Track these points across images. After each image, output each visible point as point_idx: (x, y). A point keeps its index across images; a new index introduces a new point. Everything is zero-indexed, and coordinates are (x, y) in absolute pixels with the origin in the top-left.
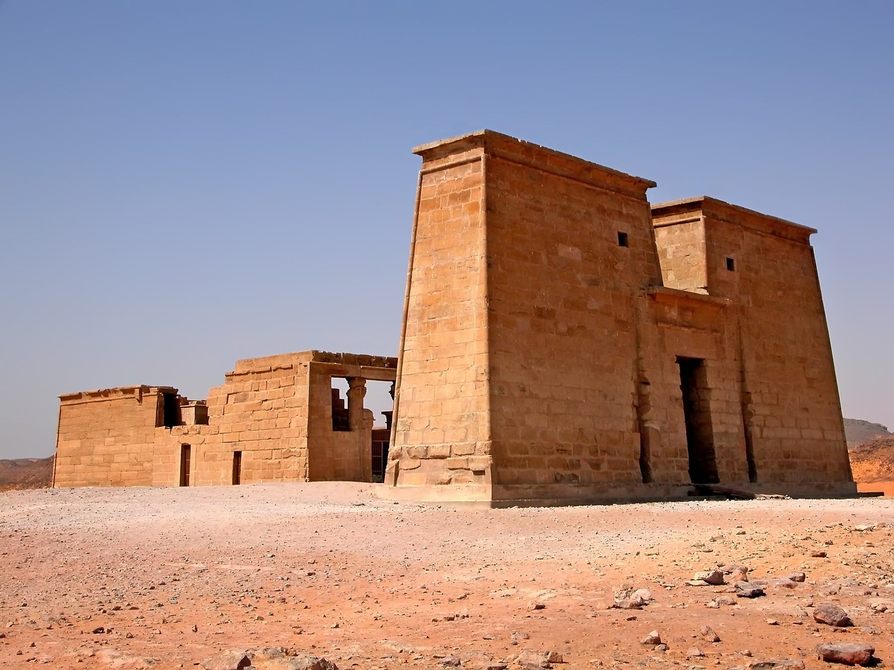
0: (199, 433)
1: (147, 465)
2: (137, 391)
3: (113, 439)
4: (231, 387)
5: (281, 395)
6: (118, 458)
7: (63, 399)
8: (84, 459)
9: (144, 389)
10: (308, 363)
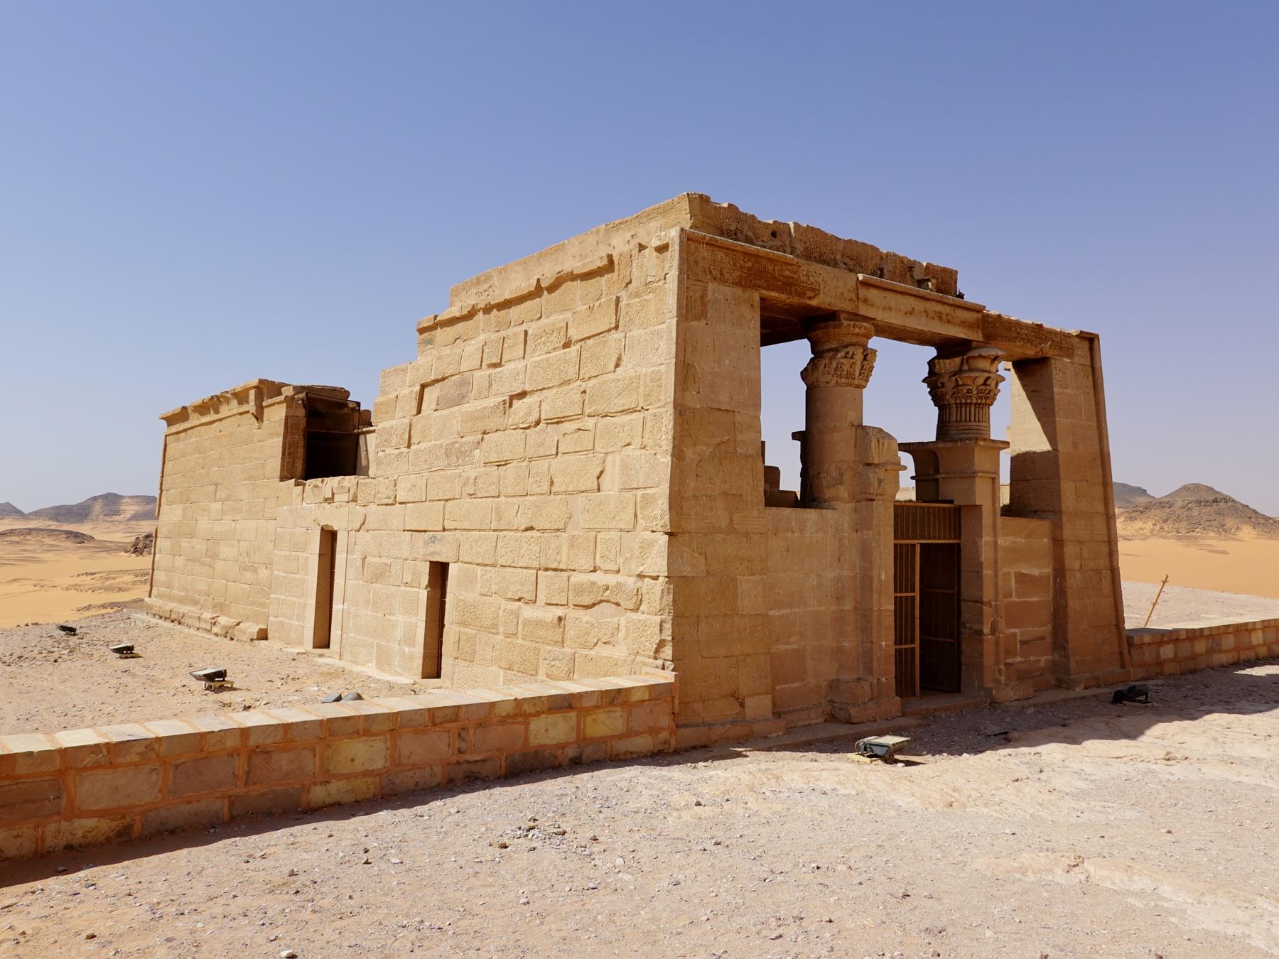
0: (354, 500)
2: (252, 393)
3: (216, 506)
4: (427, 363)
5: (572, 372)
6: (226, 551)
7: (171, 420)
8: (185, 544)
9: (267, 390)
10: (674, 233)
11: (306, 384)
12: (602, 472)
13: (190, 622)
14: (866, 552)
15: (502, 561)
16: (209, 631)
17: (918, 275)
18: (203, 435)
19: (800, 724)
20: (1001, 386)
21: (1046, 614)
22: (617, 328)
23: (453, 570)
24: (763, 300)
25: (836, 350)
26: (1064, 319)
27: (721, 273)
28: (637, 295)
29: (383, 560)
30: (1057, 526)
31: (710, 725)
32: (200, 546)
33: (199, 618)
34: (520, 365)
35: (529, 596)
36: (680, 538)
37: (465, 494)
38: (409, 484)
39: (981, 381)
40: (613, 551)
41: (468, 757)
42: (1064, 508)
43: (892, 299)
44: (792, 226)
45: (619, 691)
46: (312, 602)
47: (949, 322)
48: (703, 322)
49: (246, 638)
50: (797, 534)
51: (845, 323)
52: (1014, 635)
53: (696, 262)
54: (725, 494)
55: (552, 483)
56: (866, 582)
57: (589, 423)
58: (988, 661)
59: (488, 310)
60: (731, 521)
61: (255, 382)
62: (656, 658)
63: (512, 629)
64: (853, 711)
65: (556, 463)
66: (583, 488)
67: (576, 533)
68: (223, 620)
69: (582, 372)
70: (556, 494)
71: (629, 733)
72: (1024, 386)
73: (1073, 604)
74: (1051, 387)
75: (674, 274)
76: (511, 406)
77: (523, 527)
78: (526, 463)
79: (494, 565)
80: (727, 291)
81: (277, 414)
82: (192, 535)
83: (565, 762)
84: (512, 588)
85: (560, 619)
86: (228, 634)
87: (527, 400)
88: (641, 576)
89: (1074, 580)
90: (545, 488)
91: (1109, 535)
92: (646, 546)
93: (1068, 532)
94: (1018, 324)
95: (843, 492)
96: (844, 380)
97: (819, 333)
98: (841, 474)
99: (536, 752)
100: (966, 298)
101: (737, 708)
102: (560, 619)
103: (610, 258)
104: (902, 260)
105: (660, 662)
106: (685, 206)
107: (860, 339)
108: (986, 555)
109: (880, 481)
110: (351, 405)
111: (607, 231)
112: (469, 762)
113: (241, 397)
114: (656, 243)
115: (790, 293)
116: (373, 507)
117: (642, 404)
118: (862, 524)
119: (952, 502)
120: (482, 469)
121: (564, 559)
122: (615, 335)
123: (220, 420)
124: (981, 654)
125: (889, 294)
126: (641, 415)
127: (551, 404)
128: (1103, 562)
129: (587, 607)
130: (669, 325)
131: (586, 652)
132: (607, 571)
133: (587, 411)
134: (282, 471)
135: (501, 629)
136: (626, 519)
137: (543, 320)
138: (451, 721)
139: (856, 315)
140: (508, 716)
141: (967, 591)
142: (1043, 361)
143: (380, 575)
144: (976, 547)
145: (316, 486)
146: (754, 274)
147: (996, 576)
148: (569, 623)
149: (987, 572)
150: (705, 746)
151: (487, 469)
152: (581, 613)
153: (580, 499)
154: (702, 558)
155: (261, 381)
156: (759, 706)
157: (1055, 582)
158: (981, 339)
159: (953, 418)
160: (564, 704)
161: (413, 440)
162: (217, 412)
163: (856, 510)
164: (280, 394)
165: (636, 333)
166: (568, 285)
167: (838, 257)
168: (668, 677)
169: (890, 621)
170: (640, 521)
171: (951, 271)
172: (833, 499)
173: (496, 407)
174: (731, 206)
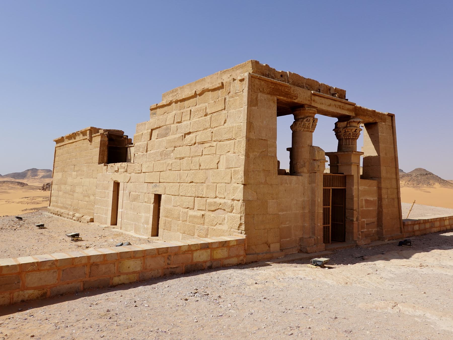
0: (126, 171)
1: (92, 198)
2: (88, 132)
3: (75, 173)
4: (153, 121)
5: (208, 125)
6: (78, 189)
7: (57, 142)
8: (63, 187)
9: (94, 131)
10: (246, 75)
11: (108, 129)
12: (219, 162)
13: (65, 215)
14: (313, 192)
15: (181, 194)
16: (72, 219)
17: (332, 92)
18: (70, 148)
19: (290, 253)
20: (361, 132)
21: (375, 214)
22: (225, 109)
23: (163, 197)
24: (278, 100)
25: (303, 118)
26: (383, 109)
27: (263, 90)
28: (232, 97)
29: (137, 193)
30: (379, 183)
31: (258, 254)
32: (68, 188)
33: (68, 214)
34: (188, 122)
35: (191, 207)
36: (248, 186)
37: (168, 169)
38: (147, 166)
39: (354, 130)
40: (223, 191)
41: (171, 266)
42: (382, 176)
43: (324, 100)
44: (288, 73)
45: (226, 242)
46: (110, 208)
47: (343, 109)
48: (257, 107)
49: (86, 221)
50: (289, 185)
51: (307, 109)
52: (364, 221)
53: (254, 85)
54: (264, 170)
55: (200, 165)
56: (313, 202)
57: (214, 144)
58: (355, 230)
59: (176, 102)
60: (266, 180)
61: (89, 128)
62: (238, 230)
63: (185, 219)
64: (308, 249)
65: (202, 158)
66: (212, 168)
67: (209, 184)
68: (77, 215)
69: (212, 125)
70: (202, 170)
71: (229, 257)
72: (368, 132)
73: (385, 211)
74: (378, 133)
75: (246, 89)
76: (185, 137)
77: (189, 181)
78: (190, 158)
79: (178, 195)
80: (265, 96)
81: (97, 140)
82: (65, 184)
83: (206, 268)
84: (185, 204)
85: (203, 215)
86: (79, 220)
87: (191, 135)
88: (233, 200)
89: (385, 202)
90: (198, 167)
91: (397, 186)
92: (235, 189)
93: (383, 185)
94: (367, 110)
95: (305, 170)
96: (306, 129)
97: (297, 112)
98: (305, 163)
99: (196, 264)
100: (349, 101)
101: (268, 248)
102: (203, 215)
103: (222, 83)
104: (327, 86)
105: (240, 231)
106: (250, 65)
107: (312, 115)
108: (355, 193)
109: (318, 166)
110: (124, 137)
111: (221, 74)
112: (171, 268)
113: (84, 133)
114: (239, 78)
115: (287, 97)
116: (133, 174)
117: (234, 137)
118: (312, 181)
119: (343, 174)
120: (174, 160)
121: (205, 193)
122: (224, 112)
123: (76, 142)
124: (353, 228)
125: (322, 98)
126: (233, 141)
127: (200, 136)
128: (395, 196)
129: (213, 211)
130: (245, 107)
131: (212, 227)
132: (220, 198)
133: (213, 139)
134: (99, 160)
135: (181, 219)
136: (228, 179)
137: (197, 106)
138: (165, 253)
139: (311, 106)
140: (186, 251)
141: (348, 205)
142: (375, 124)
143: (136, 199)
144: (351, 190)
145: (112, 166)
146: (275, 90)
147: (358, 200)
148: (206, 217)
149: (355, 199)
150: (256, 262)
151: (176, 160)
152: (210, 213)
153: (211, 171)
154: (255, 193)
155: (91, 128)
156: (275, 247)
157: (378, 203)
158: (354, 115)
159: (344, 144)
160: (206, 246)
161: (148, 150)
162: (75, 139)
163: (310, 176)
164: (98, 132)
165: (232, 111)
166: (207, 93)
167: (304, 85)
168: (243, 236)
169: (321, 216)
170: (233, 180)
172: (301, 172)
173: (179, 137)
174: (266, 65)
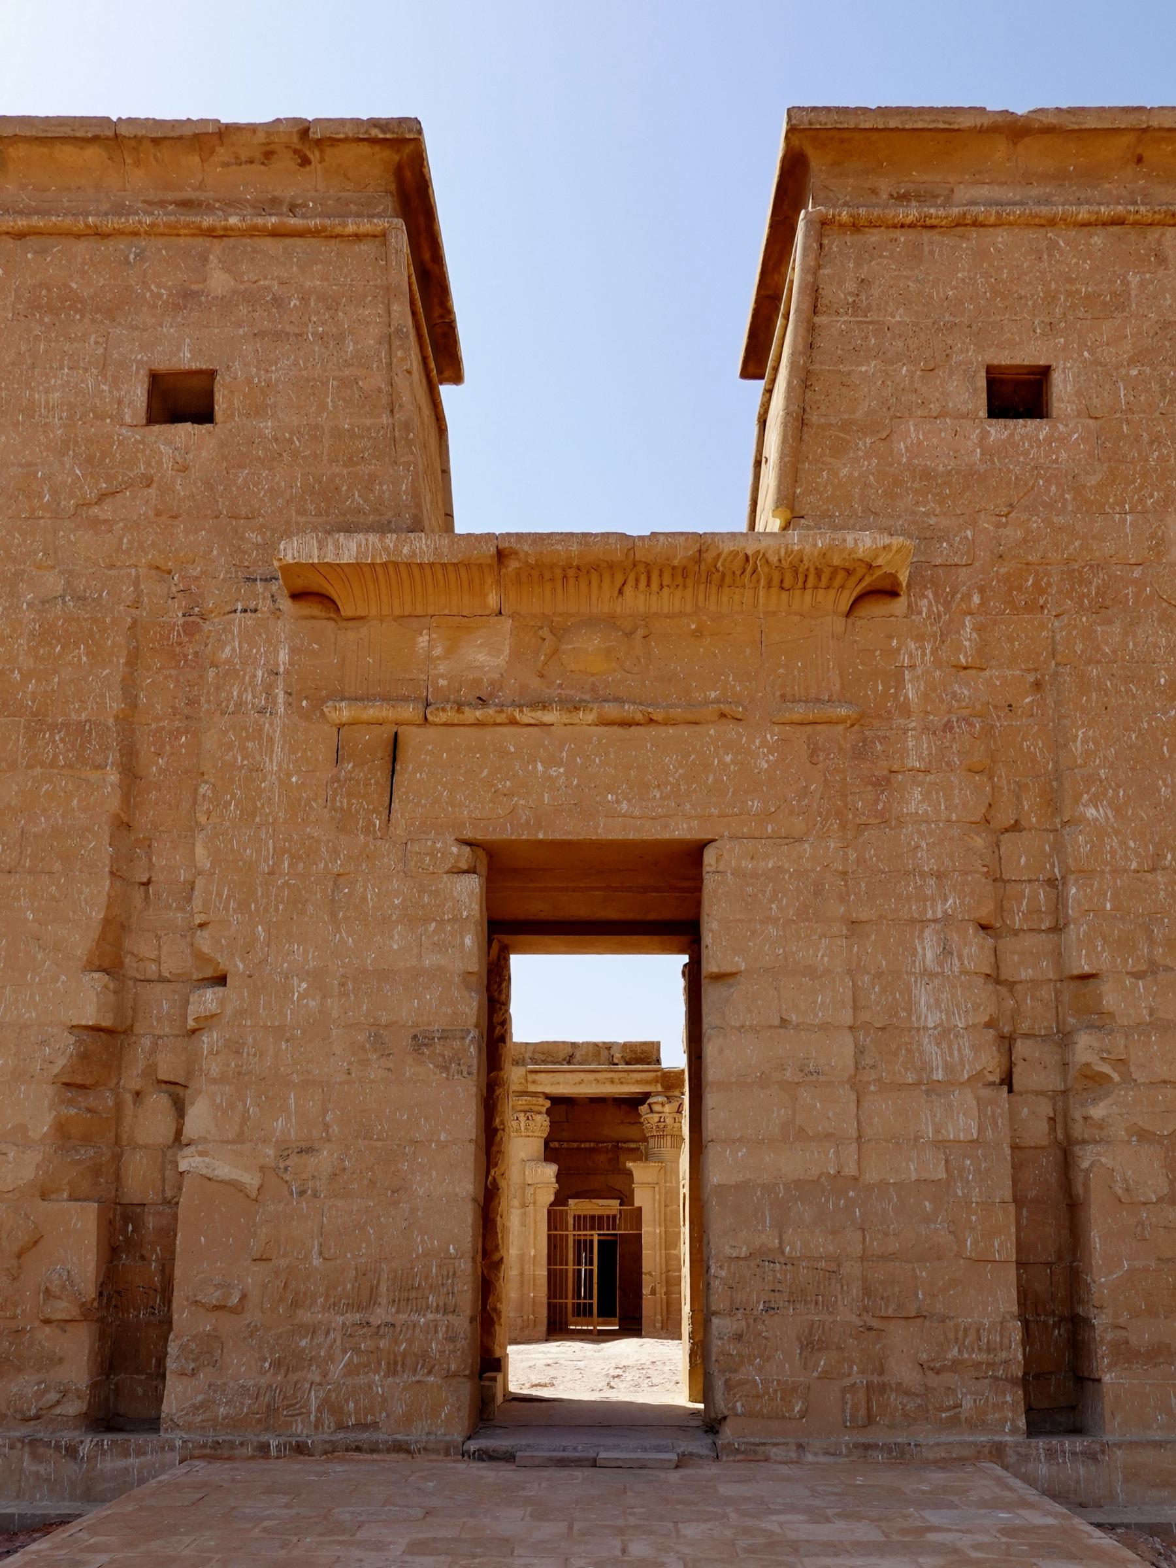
39: (657, 1120)
43: (560, 1077)
104: (596, 1044)
167: (527, 1056)
171: (653, 1043)
